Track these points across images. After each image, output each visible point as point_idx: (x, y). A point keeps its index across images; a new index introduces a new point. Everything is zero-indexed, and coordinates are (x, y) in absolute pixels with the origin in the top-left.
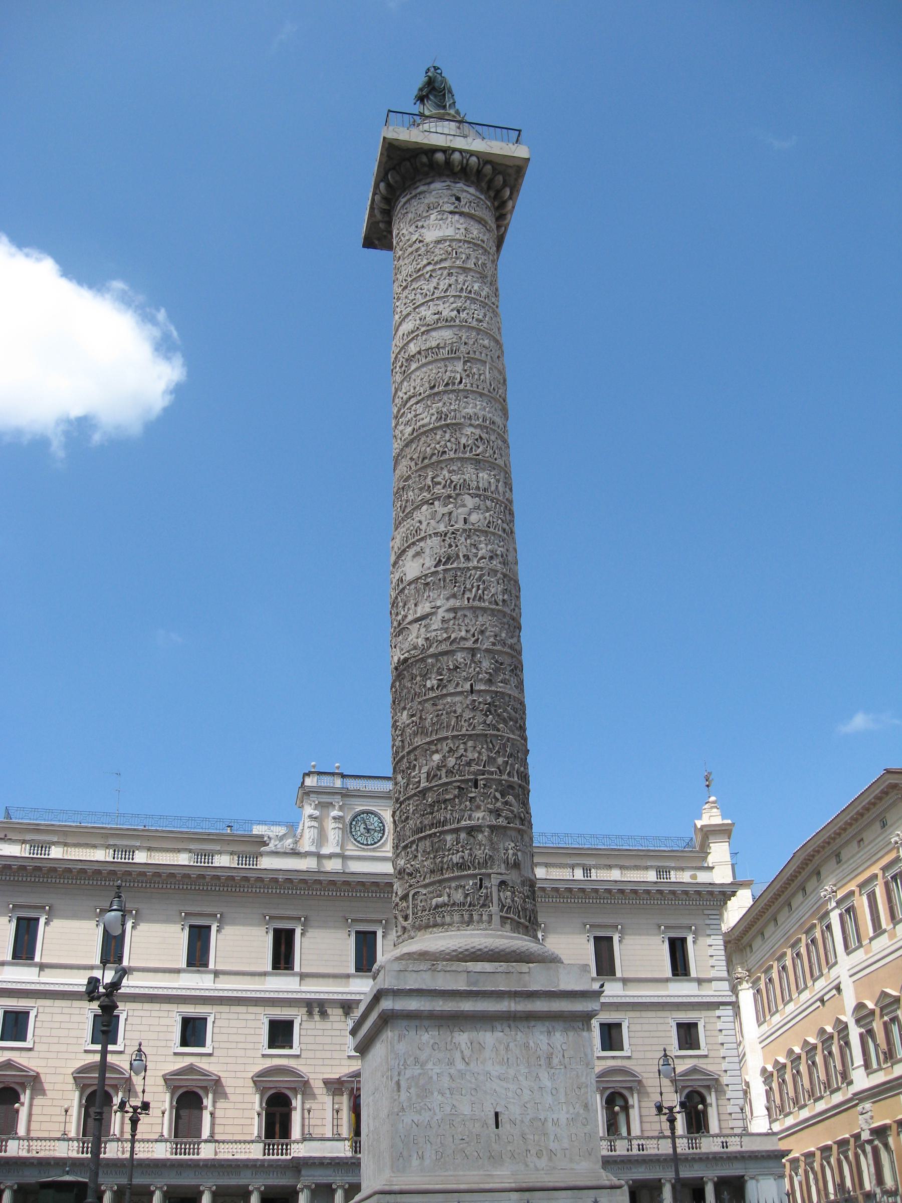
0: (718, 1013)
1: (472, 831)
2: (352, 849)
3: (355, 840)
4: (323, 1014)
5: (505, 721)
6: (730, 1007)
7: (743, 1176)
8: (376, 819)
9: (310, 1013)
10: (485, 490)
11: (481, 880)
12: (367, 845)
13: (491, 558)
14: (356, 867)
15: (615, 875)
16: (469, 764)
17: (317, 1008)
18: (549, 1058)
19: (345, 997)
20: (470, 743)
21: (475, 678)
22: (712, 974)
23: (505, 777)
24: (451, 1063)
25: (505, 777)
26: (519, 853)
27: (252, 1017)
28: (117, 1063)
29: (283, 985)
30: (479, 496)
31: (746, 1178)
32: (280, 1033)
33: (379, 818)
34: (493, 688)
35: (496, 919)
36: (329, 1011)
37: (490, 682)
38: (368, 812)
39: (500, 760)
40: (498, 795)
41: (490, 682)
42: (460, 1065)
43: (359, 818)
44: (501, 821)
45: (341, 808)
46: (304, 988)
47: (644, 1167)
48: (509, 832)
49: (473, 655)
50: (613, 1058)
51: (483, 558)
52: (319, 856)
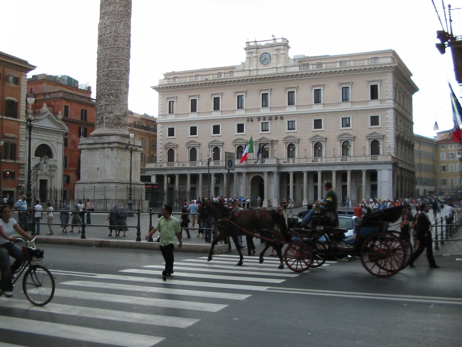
0: (387, 112)
1: (101, 106)
2: (261, 67)
3: (261, 63)
4: (252, 121)
5: (111, 77)
6: (392, 109)
7: (376, 169)
8: (268, 55)
9: (248, 121)
10: (111, 12)
11: (102, 117)
12: (265, 64)
13: (111, 33)
14: (261, 73)
15: (352, 64)
16: (101, 90)
17: (250, 119)
18: (108, 156)
19: (258, 115)
20: (102, 85)
21: (104, 68)
22: (387, 97)
23: (110, 92)
24: (91, 158)
25: (110, 92)
26: (112, 110)
27: (232, 124)
28: (197, 140)
29: (241, 113)
30: (109, 15)
31: (377, 170)
32: (240, 128)
33: (269, 54)
34: (109, 69)
35: (104, 126)
36: (254, 121)
37: (107, 68)
38: (265, 53)
39: (108, 88)
40: (107, 97)
41: (107, 68)
42: (92, 159)
43: (263, 55)
44: (108, 103)
45: (257, 53)
46: (246, 114)
47: (341, 166)
48: (110, 105)
49: (104, 61)
50: (346, 129)
51: (108, 34)
52: (250, 70)
